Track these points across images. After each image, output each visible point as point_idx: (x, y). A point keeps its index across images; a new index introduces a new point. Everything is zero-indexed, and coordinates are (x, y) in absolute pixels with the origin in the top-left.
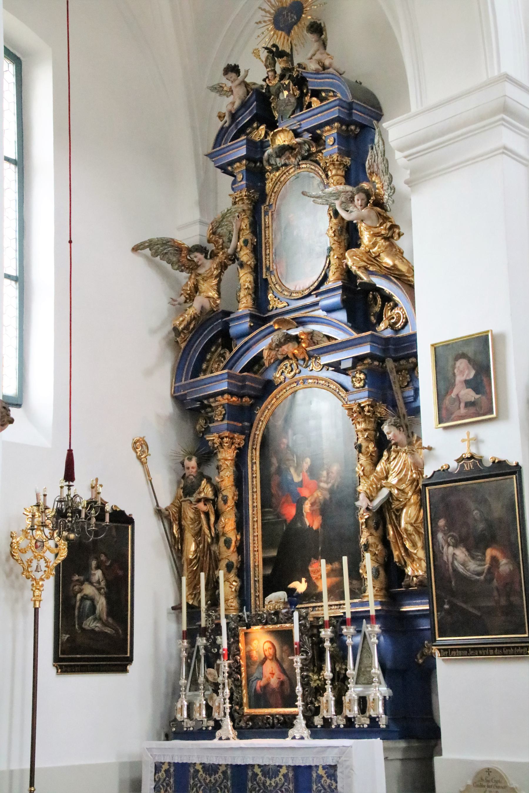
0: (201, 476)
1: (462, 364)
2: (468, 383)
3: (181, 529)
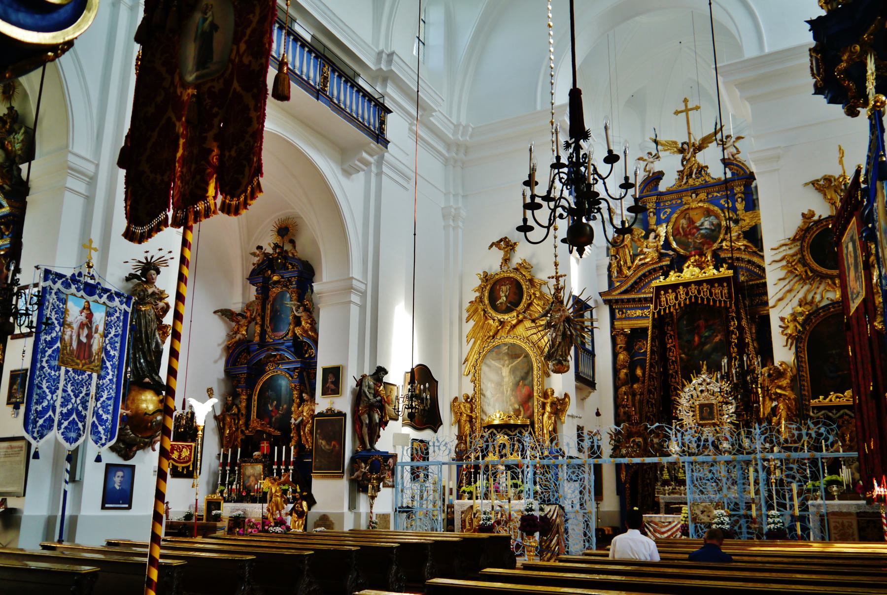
0: (233, 404)
1: (331, 375)
2: (332, 383)
3: (224, 424)
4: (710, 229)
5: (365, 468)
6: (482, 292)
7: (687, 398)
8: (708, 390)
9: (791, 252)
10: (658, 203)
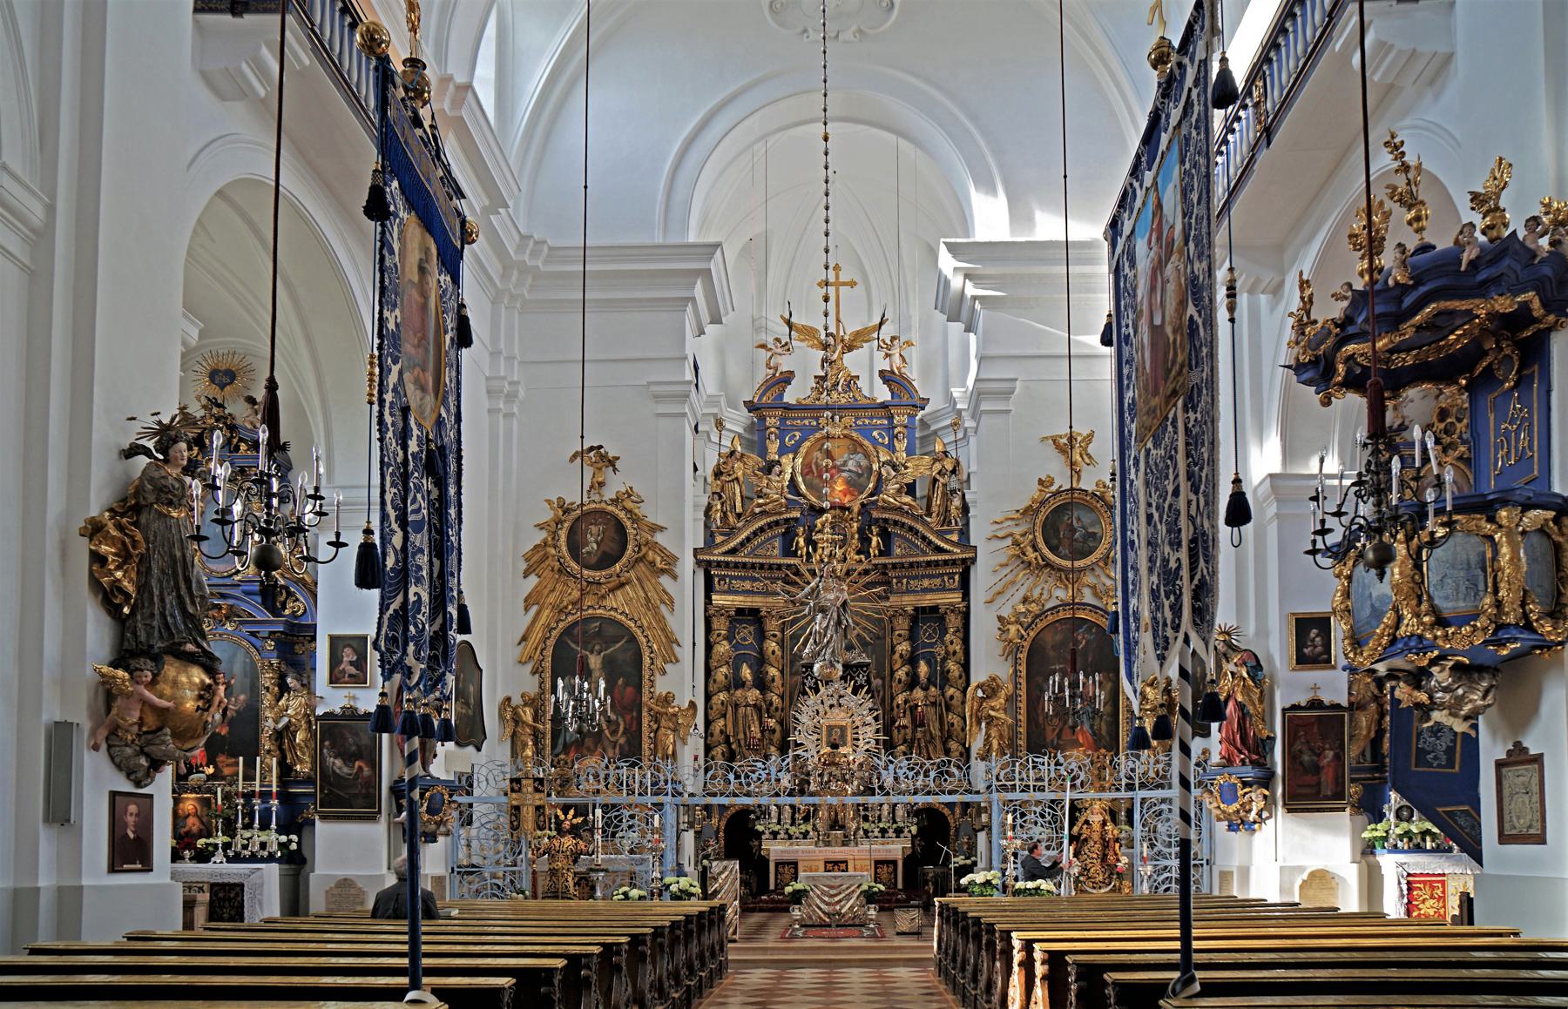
2: (351, 663)
4: (857, 473)
6: (554, 535)
7: (811, 713)
8: (840, 705)
9: (1018, 531)
10: (783, 419)
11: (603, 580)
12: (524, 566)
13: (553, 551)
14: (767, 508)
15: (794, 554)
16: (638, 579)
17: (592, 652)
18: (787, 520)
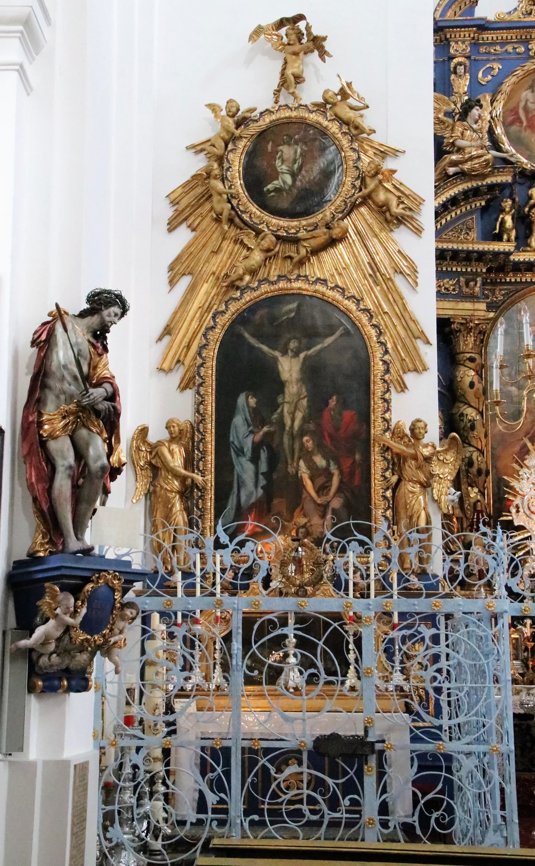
5: (74, 614)
10: (475, 44)
11: (302, 234)
12: (169, 212)
13: (219, 185)
14: (466, 167)
15: (498, 238)
16: (358, 233)
17: (284, 353)
18: (491, 187)
